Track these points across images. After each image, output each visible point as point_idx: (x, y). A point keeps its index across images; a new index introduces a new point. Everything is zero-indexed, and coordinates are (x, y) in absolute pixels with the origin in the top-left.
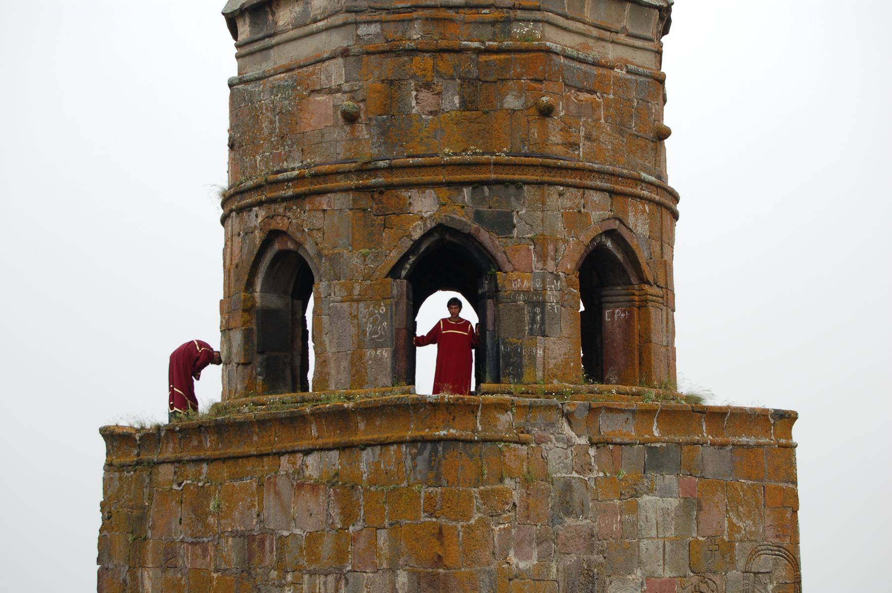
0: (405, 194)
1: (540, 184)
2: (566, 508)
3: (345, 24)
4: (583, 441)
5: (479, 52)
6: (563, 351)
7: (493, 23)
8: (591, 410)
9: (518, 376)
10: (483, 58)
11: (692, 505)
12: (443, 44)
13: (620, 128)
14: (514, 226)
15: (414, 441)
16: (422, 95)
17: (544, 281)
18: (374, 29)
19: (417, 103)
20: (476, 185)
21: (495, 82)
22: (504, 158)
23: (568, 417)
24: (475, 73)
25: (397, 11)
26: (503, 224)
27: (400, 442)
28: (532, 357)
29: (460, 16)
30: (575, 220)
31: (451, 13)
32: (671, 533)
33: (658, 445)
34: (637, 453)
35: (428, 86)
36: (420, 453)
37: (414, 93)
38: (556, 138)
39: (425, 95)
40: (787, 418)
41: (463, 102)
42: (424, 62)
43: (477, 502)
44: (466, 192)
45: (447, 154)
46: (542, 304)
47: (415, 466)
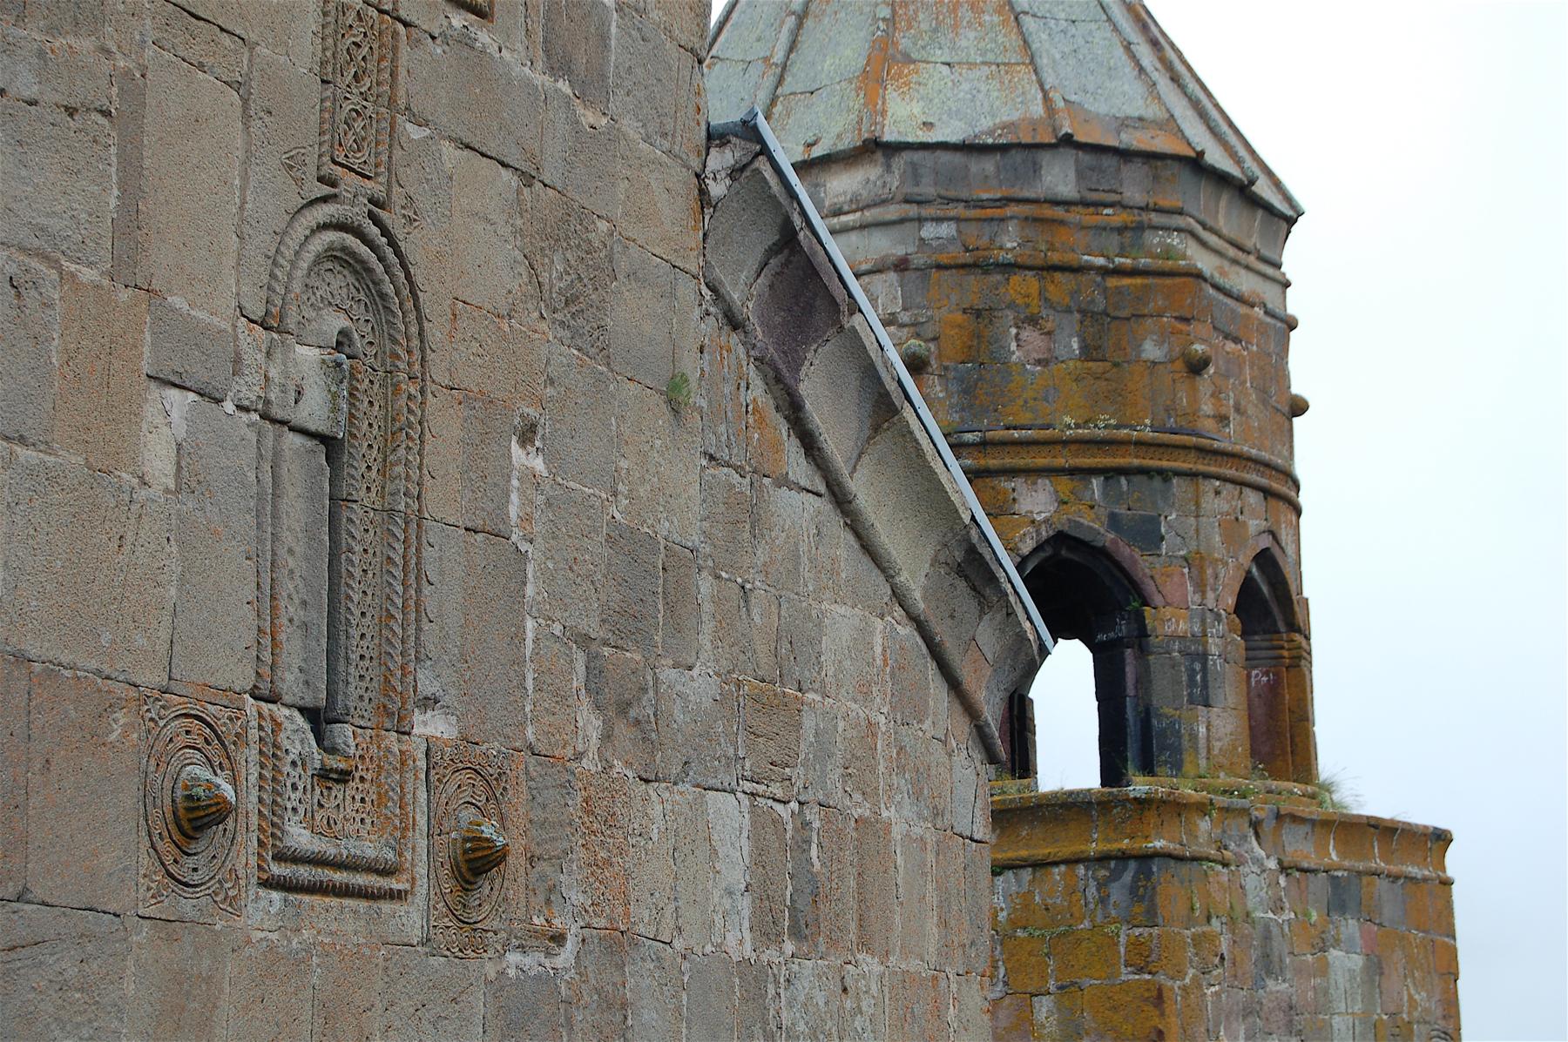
0: (1006, 484)
1: (1192, 475)
2: (1269, 966)
3: (902, 221)
4: (1272, 864)
5: (1105, 272)
6: (1229, 728)
7: (1121, 230)
8: (1279, 817)
9: (1177, 766)
10: (1112, 282)
11: (1375, 968)
12: (1055, 258)
13: (1263, 392)
14: (1162, 538)
15: (1103, 859)
16: (1024, 335)
17: (1203, 621)
18: (946, 230)
19: (1021, 347)
20: (1110, 474)
21: (1128, 319)
22: (1148, 434)
23: (1256, 825)
24: (1101, 304)
25: (980, 204)
26: (1149, 536)
27: (1072, 862)
28: (1194, 737)
29: (1075, 216)
30: (1233, 527)
31: (1059, 212)
32: (1358, 1008)
33: (1340, 874)
34: (1319, 883)
35: (1033, 321)
36: (1115, 876)
37: (1014, 331)
38: (1207, 408)
39: (1028, 334)
40: (1442, 839)
41: (1084, 348)
42: (1024, 286)
43: (1190, 952)
44: (1096, 483)
45: (1068, 423)
46: (1203, 657)
47: (1103, 901)
